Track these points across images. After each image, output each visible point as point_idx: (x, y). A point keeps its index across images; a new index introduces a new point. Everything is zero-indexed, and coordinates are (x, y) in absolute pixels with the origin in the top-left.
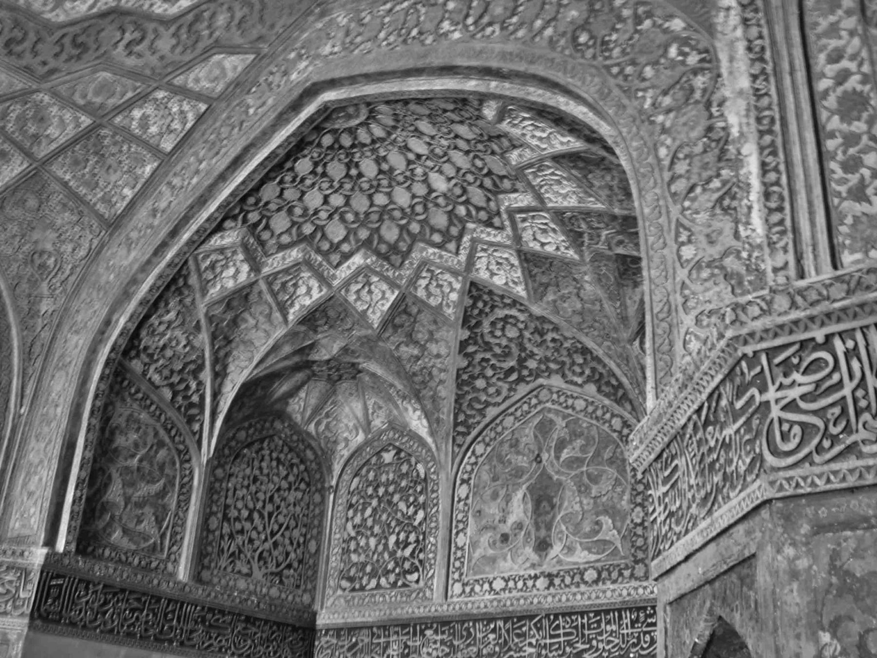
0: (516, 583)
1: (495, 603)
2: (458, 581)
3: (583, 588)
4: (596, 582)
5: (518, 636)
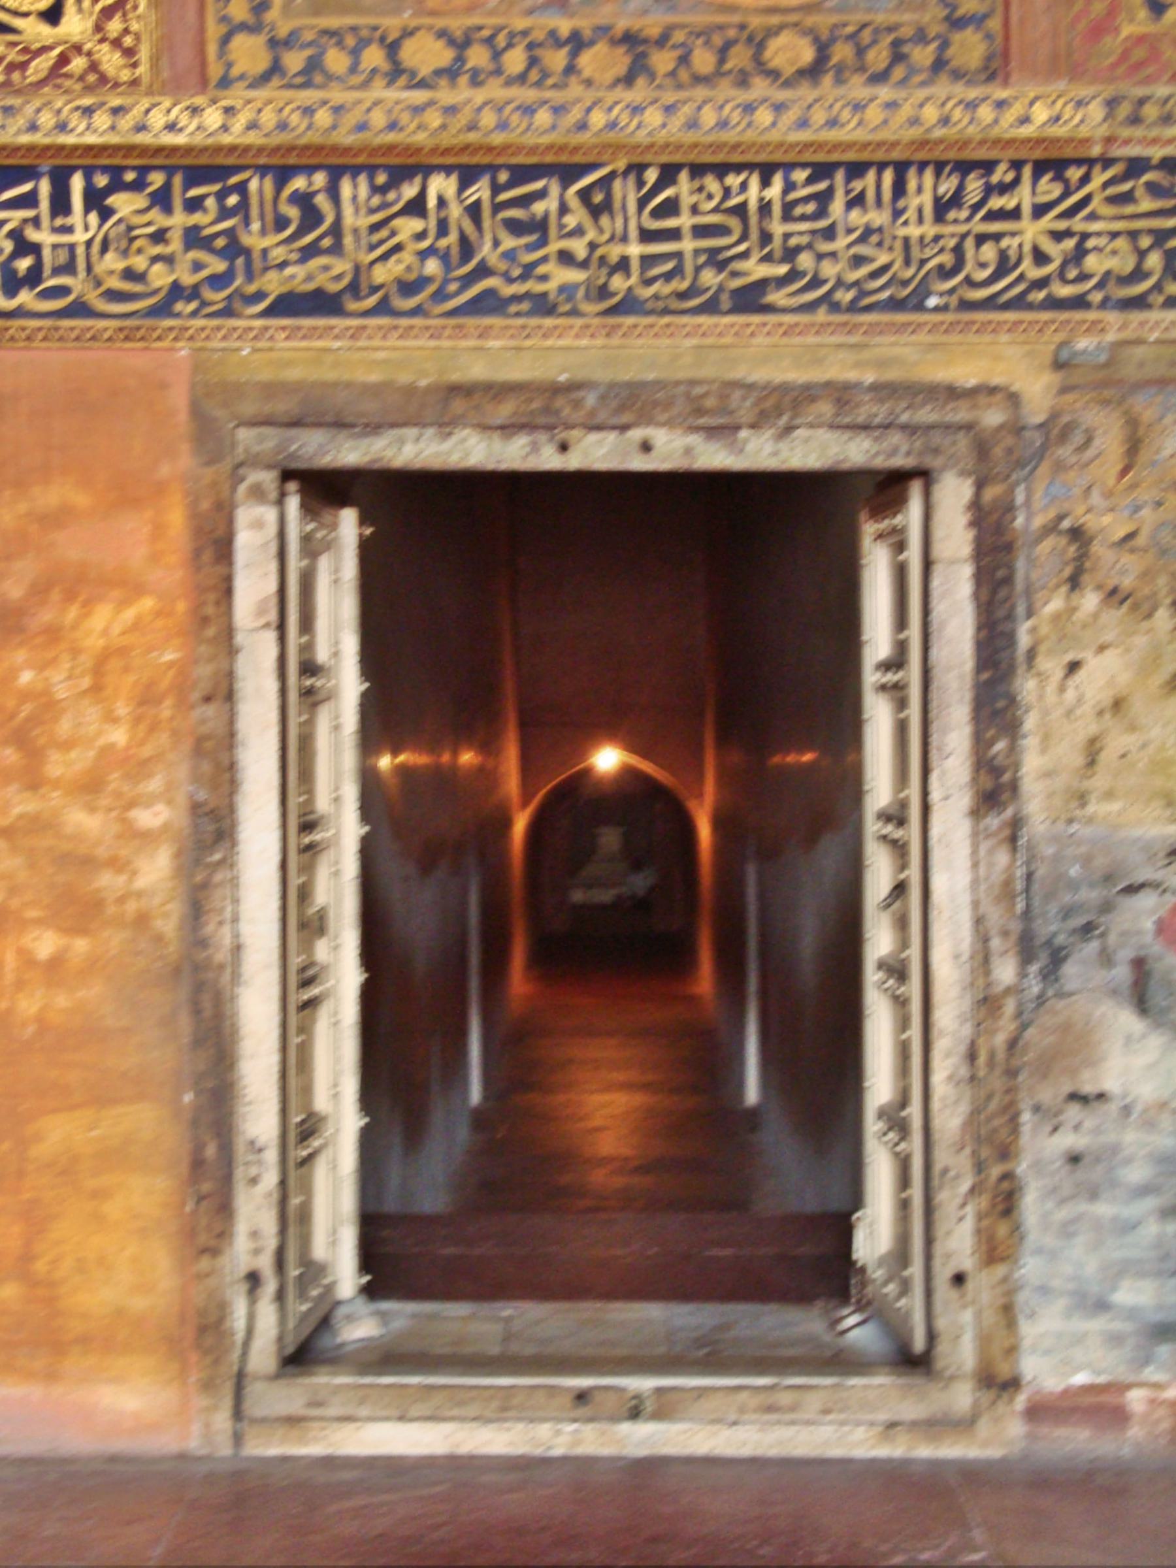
0: (497, 55)
1: (434, 119)
2: (243, 27)
3: (760, 87)
4: (813, 72)
5: (515, 227)
